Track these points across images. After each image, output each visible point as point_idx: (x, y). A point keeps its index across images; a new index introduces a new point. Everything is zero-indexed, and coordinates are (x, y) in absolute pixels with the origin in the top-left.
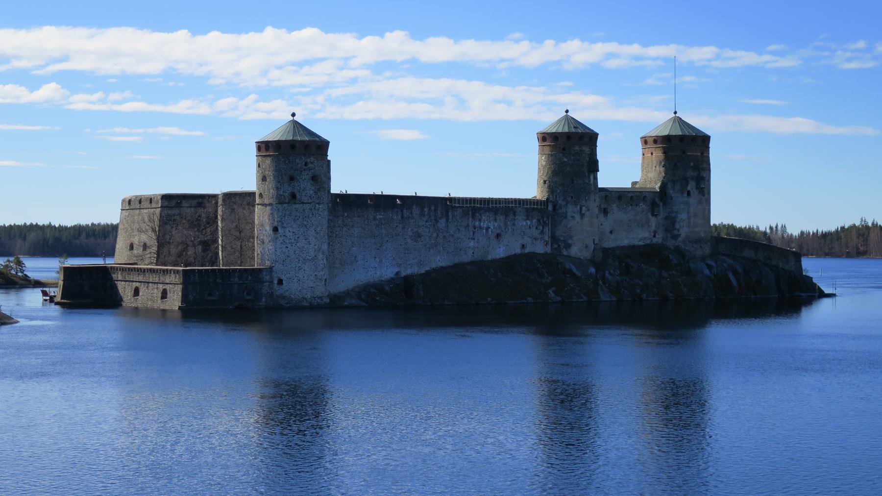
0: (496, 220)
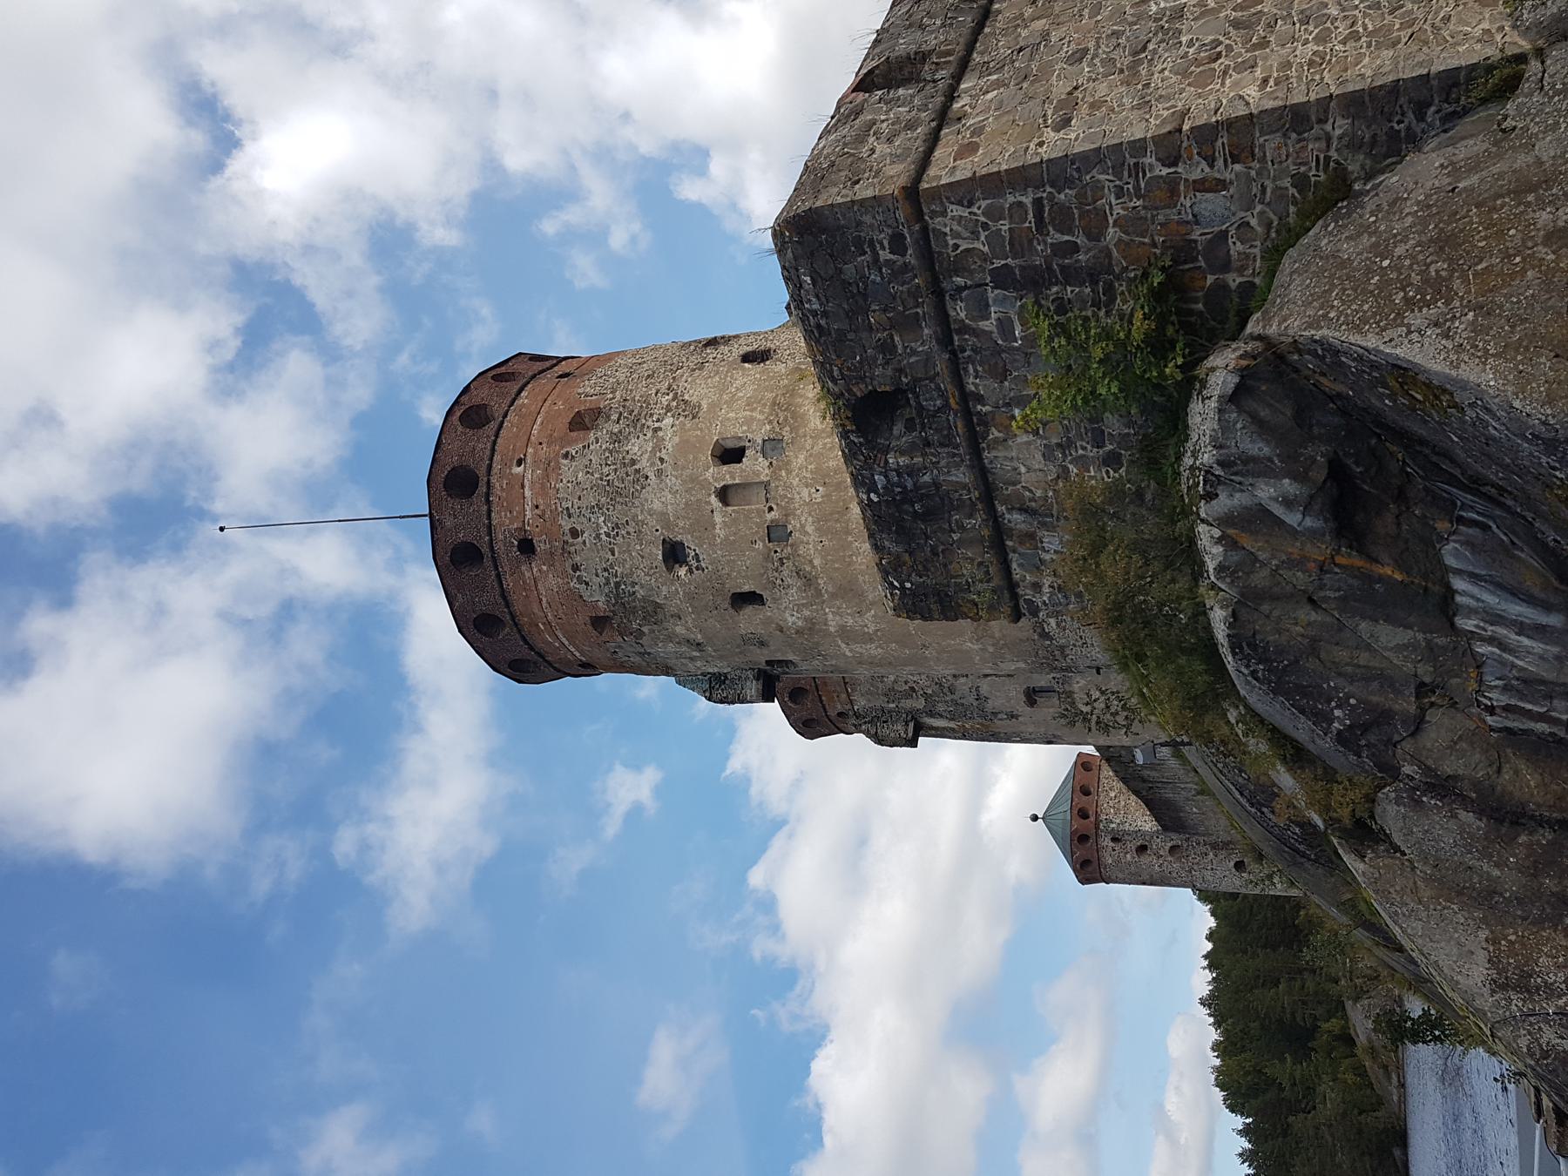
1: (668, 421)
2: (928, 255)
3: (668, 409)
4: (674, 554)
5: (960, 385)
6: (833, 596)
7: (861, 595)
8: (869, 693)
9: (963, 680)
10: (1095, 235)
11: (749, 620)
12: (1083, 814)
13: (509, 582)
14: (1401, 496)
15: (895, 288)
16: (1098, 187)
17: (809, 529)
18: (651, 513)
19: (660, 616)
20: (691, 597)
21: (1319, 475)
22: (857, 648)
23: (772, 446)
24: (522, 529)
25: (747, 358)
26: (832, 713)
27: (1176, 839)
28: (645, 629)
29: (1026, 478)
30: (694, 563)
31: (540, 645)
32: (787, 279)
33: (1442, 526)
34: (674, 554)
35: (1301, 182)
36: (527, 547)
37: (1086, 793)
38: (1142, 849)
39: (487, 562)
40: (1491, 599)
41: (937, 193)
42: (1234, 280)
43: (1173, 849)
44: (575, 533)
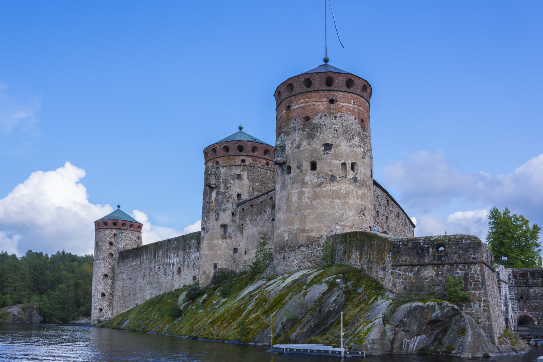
0: (177, 256)
1: (362, 150)
2: (471, 263)
3: (365, 150)
4: (328, 147)
5: (446, 264)
6: (314, 192)
7: (314, 199)
8: (226, 174)
9: (231, 205)
10: (473, 289)
11: (306, 165)
12: (124, 224)
14: (432, 329)
15: (466, 256)
16: (481, 290)
17: (334, 188)
18: (340, 142)
19: (309, 139)
20: (316, 149)
21: (440, 319)
23: (355, 180)
24: (337, 101)
26: (218, 159)
27: (116, 256)
28: (305, 133)
29: (426, 272)
30: (326, 152)
32: (467, 236)
33: (428, 335)
34: (328, 147)
35: (479, 318)
37: (131, 226)
38: (111, 244)
40: (418, 341)
41: (482, 266)
42: (464, 308)
43: (111, 255)
44: (335, 117)
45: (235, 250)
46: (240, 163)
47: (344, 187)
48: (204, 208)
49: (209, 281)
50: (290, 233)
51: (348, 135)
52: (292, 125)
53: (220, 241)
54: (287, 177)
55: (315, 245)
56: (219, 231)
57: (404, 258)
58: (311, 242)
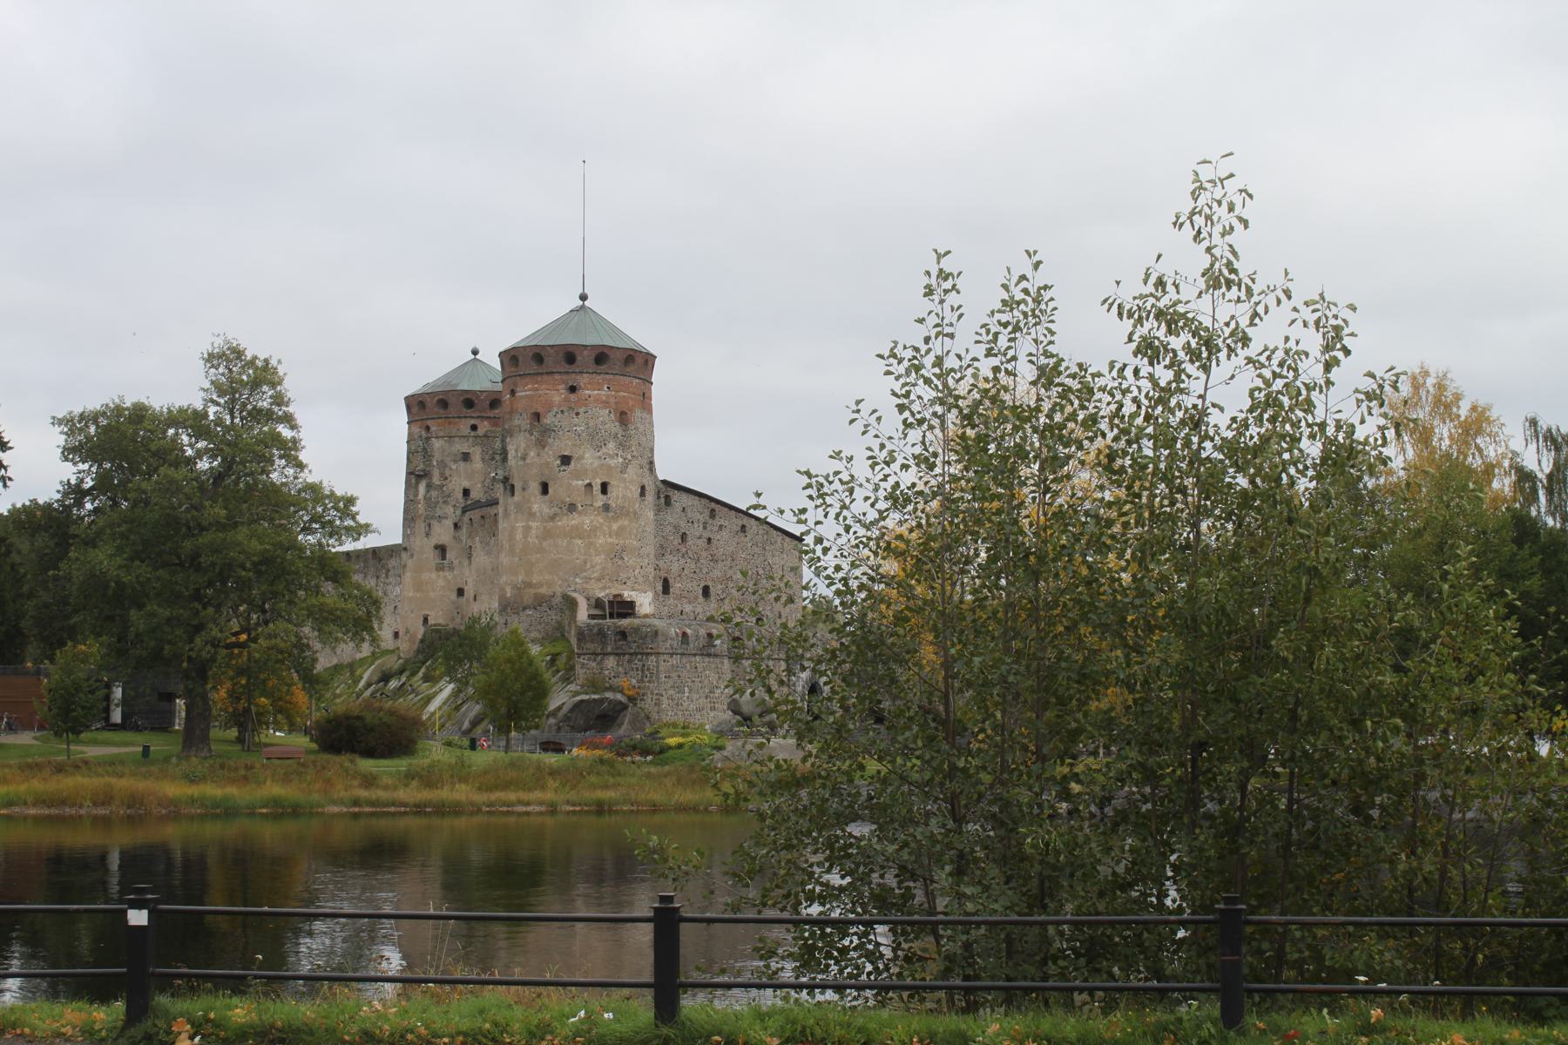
4: (566, 460)
11: (535, 487)
13: (557, 377)
20: (548, 464)
22: (520, 531)
23: (606, 508)
25: (643, 488)
26: (429, 423)
31: (528, 379)
34: (566, 460)
36: (573, 389)
39: (567, 368)
45: (461, 592)
46: (466, 430)
47: (587, 521)
48: (406, 511)
49: (415, 647)
50: (515, 587)
51: (596, 439)
52: (517, 422)
53: (434, 576)
54: (510, 500)
55: (545, 607)
56: (431, 556)
57: (588, 645)
58: (540, 602)
